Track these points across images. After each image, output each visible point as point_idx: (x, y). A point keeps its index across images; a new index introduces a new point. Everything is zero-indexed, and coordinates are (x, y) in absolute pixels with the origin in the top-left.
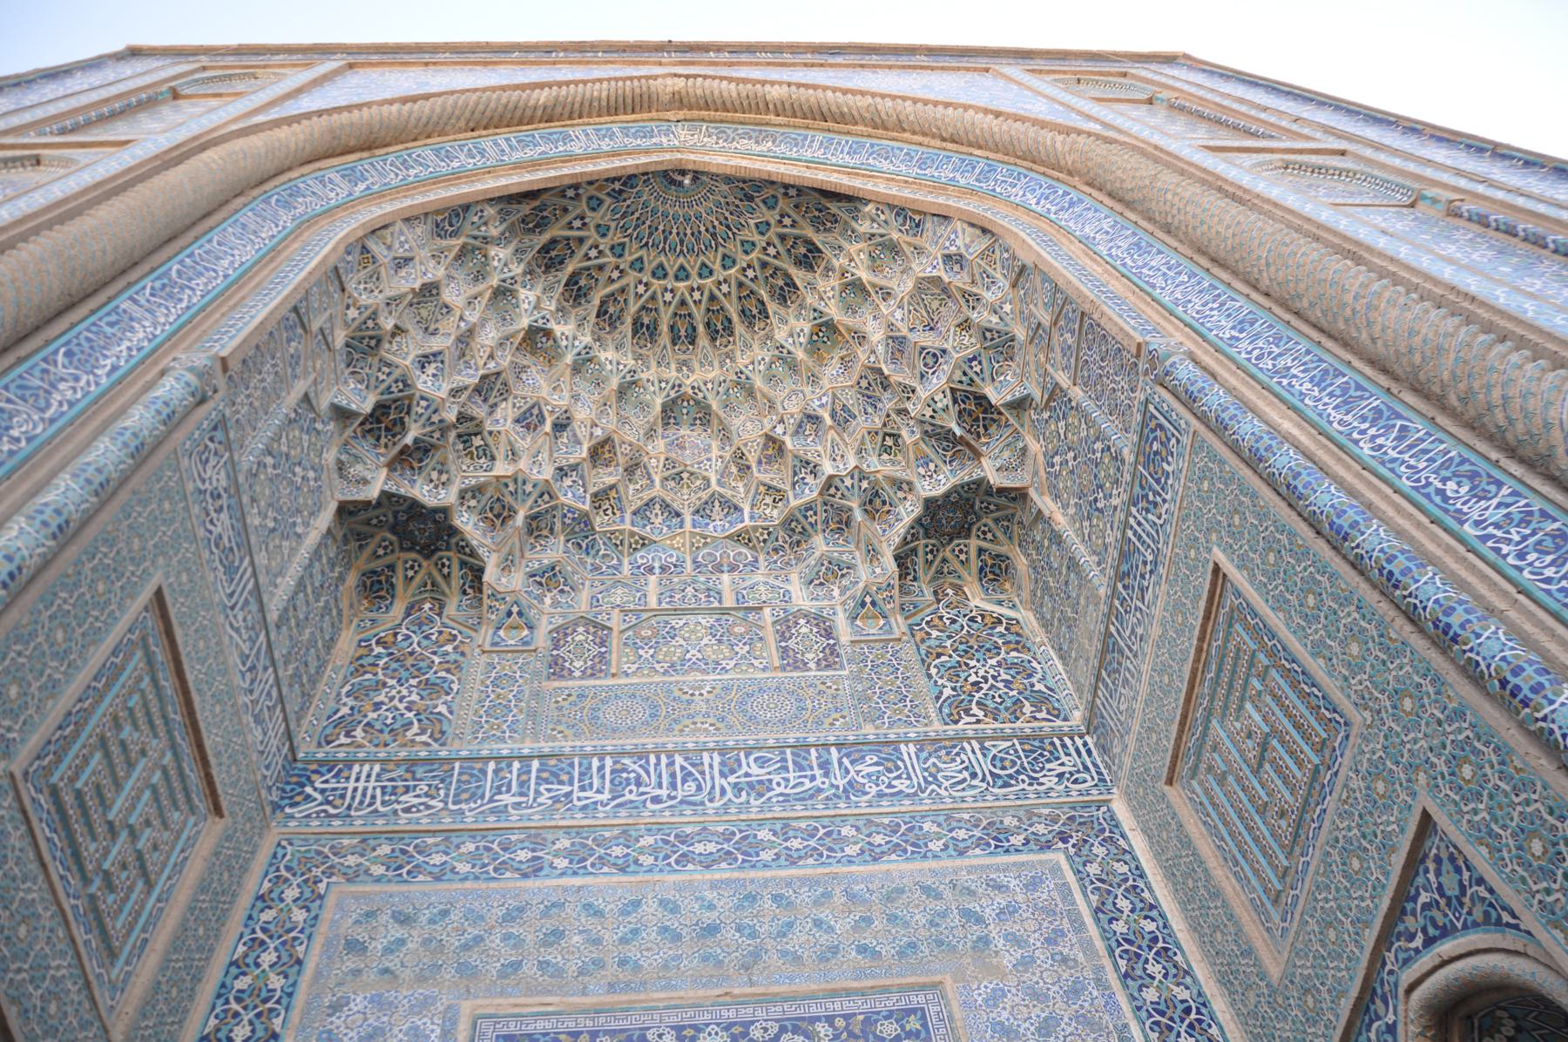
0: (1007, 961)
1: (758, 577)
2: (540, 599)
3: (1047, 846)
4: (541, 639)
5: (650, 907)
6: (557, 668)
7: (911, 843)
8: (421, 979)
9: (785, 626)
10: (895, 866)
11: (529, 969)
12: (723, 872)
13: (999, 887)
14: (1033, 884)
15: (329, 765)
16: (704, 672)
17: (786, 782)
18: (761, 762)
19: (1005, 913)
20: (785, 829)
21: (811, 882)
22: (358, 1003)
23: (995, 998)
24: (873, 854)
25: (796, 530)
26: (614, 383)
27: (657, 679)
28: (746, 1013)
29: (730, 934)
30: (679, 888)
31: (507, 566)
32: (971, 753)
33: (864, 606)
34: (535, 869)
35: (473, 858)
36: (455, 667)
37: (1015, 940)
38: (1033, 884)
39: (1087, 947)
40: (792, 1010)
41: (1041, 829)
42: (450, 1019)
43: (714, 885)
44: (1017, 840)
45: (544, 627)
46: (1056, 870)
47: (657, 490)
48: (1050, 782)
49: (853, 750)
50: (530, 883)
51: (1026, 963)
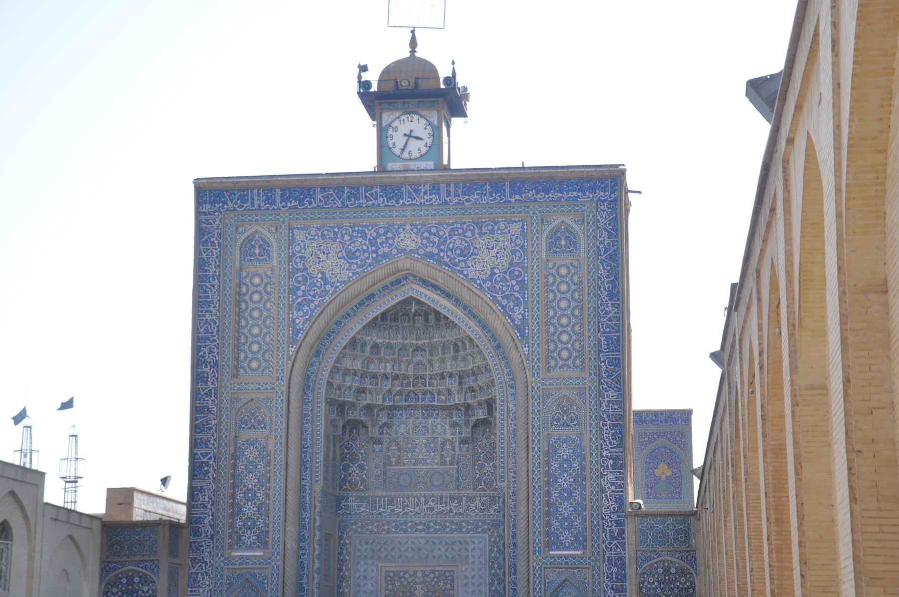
0: (470, 561)
1: (439, 421)
2: (382, 433)
3: (485, 532)
4: (385, 450)
5: (410, 543)
6: (387, 461)
7: (459, 529)
8: (371, 558)
9: (444, 443)
10: (456, 535)
11: (389, 556)
12: (423, 534)
13: (473, 542)
14: (480, 543)
15: (343, 497)
16: (423, 464)
17: (438, 508)
18: (433, 501)
19: (474, 549)
20: (436, 523)
21: (439, 538)
22: (362, 563)
23: (466, 570)
24: (451, 531)
25: (450, 408)
26: (397, 350)
27: (412, 467)
28: (425, 569)
29: (423, 550)
30: (416, 538)
31: (374, 426)
32: (478, 502)
33: (463, 441)
34: (388, 532)
35: (377, 527)
36: (365, 459)
37: (473, 557)
38: (480, 543)
39: (485, 560)
40: (433, 569)
41: (486, 527)
42: (377, 566)
43: (422, 538)
44: (480, 530)
45: (385, 444)
46: (485, 539)
47: (411, 388)
48: (492, 512)
49: (452, 499)
50: (388, 535)
51: (473, 562)
